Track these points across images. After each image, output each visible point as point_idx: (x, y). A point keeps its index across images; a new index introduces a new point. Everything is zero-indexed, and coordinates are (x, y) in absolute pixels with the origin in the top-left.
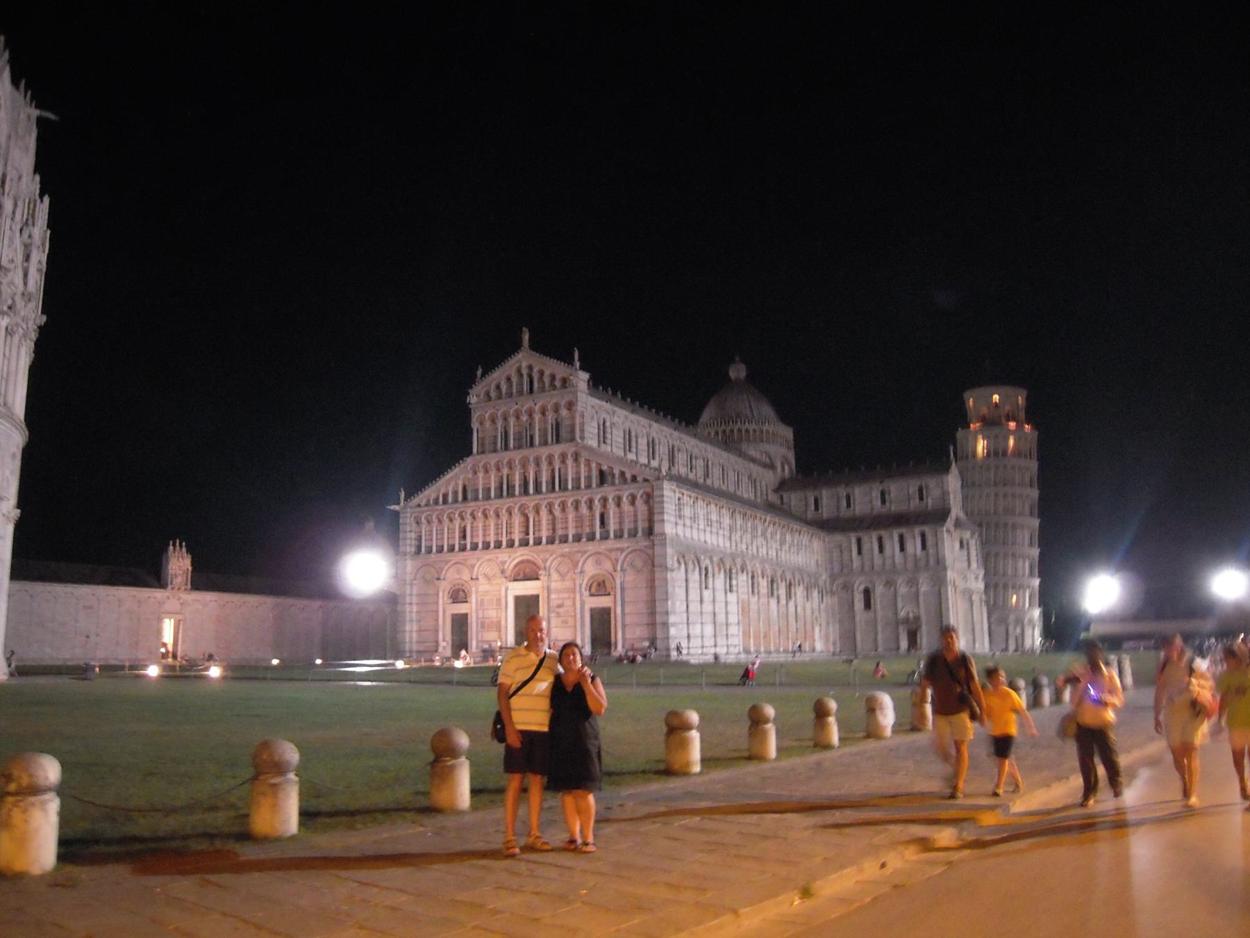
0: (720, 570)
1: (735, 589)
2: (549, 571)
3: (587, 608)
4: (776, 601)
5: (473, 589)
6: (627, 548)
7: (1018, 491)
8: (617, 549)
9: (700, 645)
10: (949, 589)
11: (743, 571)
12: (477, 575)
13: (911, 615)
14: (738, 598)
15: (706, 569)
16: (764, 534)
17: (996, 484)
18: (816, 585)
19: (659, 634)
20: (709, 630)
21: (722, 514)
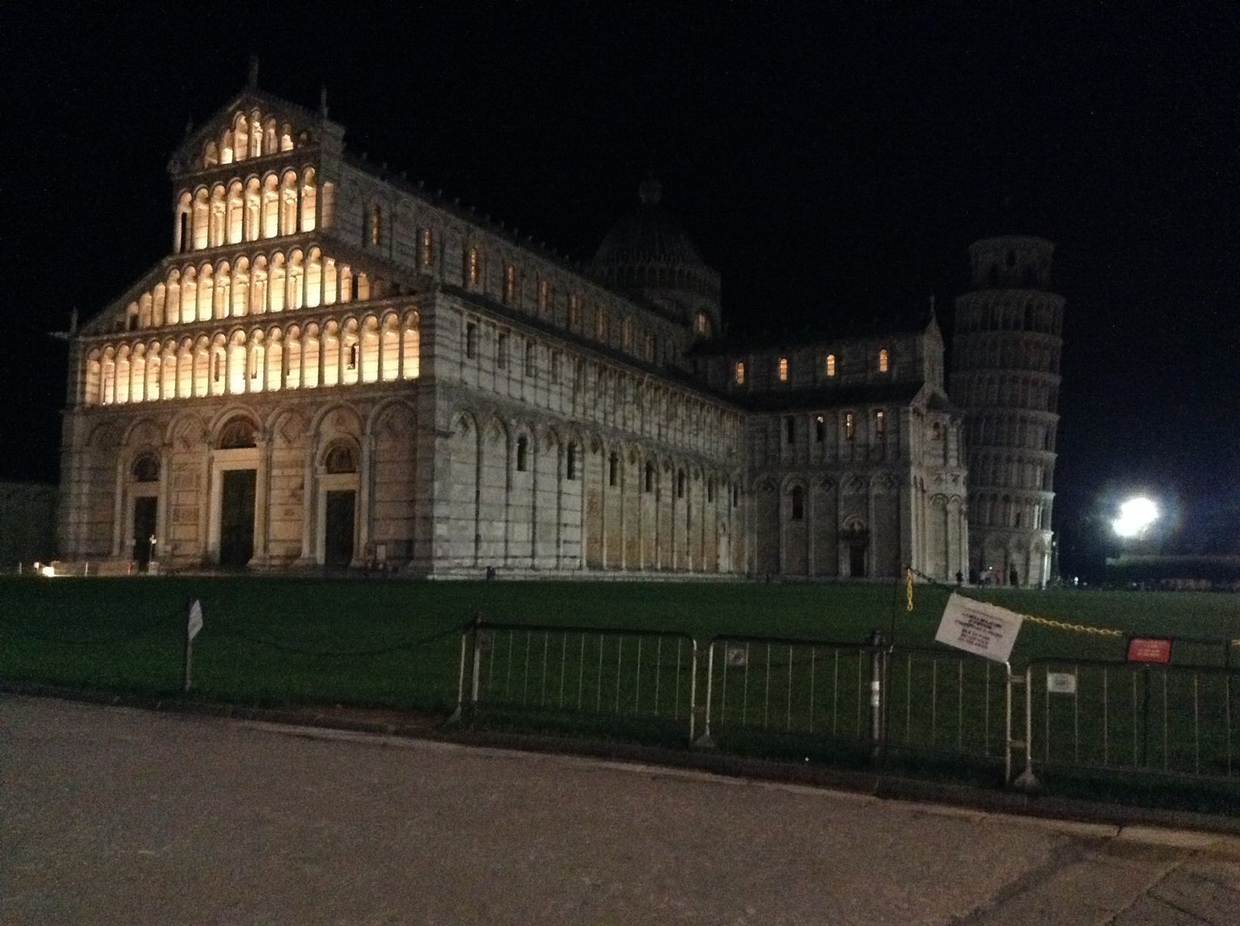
0: (551, 444)
1: (578, 474)
2: (272, 433)
3: (322, 490)
4: (654, 497)
5: (164, 461)
6: (382, 398)
7: (1034, 375)
8: (367, 401)
9: (502, 552)
10: (913, 491)
11: (595, 451)
12: (171, 438)
13: (857, 527)
14: (583, 486)
15: (522, 442)
16: (638, 401)
17: (1003, 366)
18: (725, 481)
19: (419, 533)
20: (521, 532)
21: (558, 363)
